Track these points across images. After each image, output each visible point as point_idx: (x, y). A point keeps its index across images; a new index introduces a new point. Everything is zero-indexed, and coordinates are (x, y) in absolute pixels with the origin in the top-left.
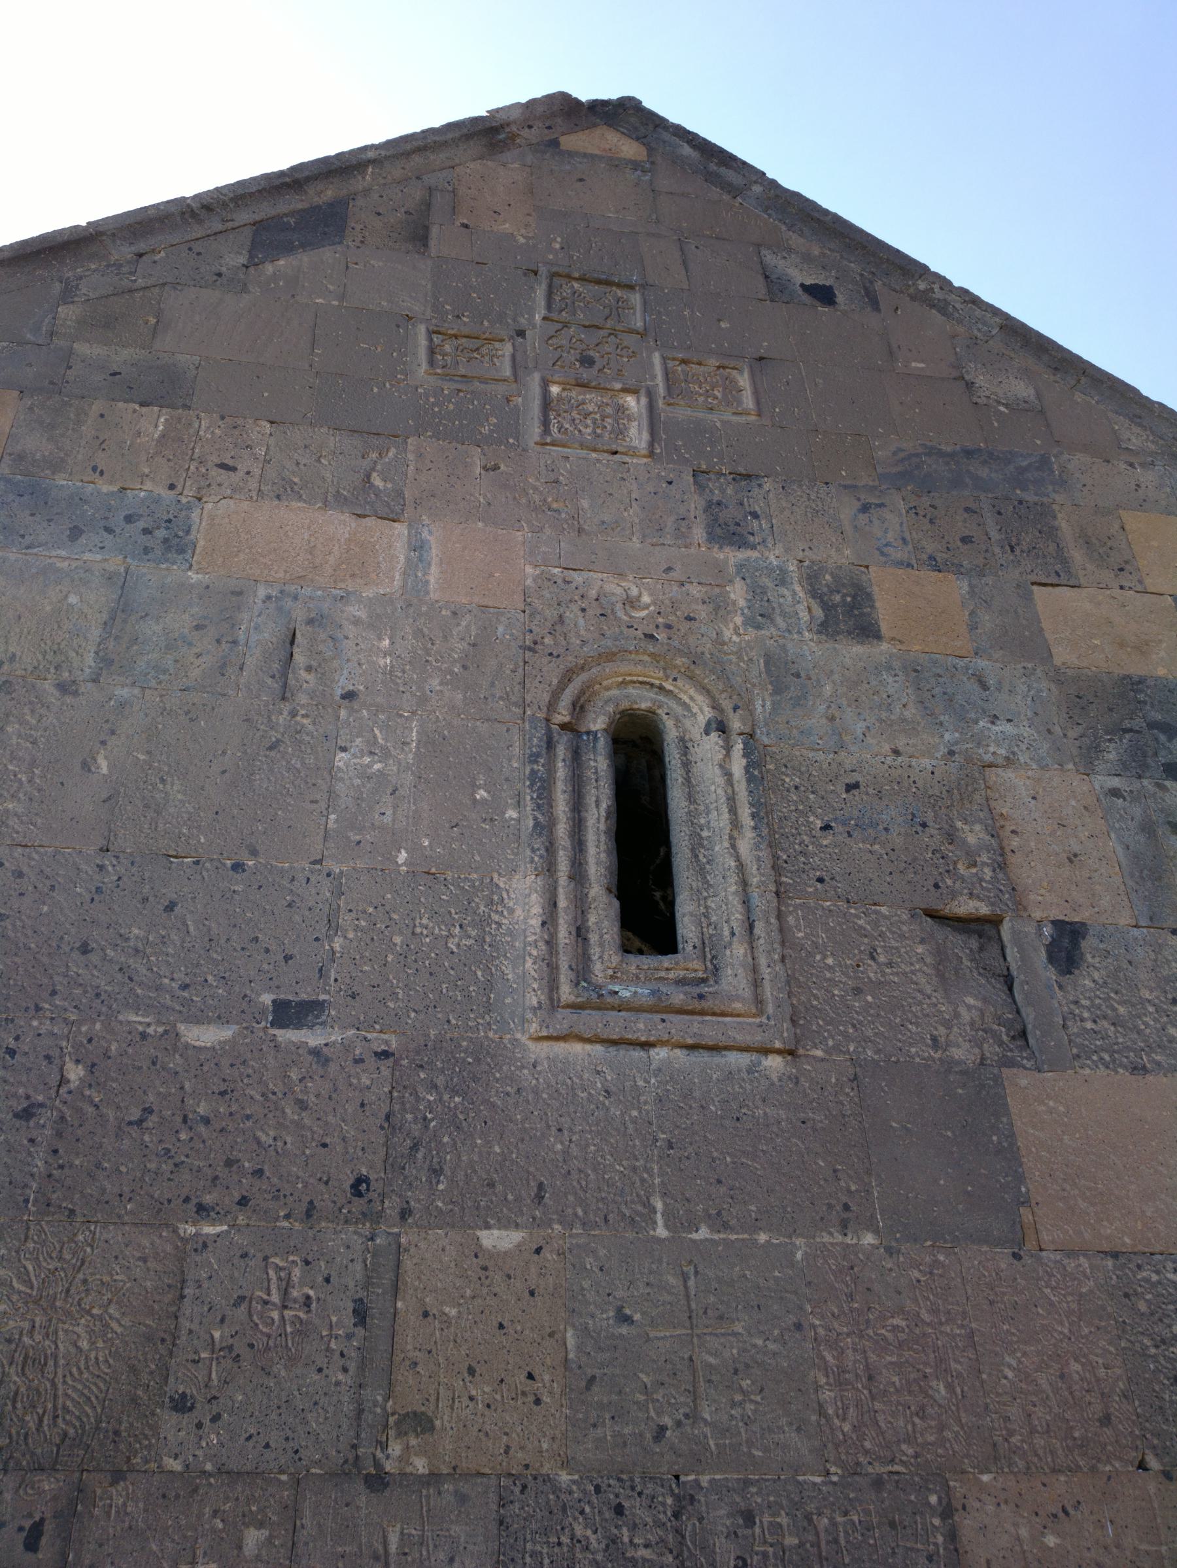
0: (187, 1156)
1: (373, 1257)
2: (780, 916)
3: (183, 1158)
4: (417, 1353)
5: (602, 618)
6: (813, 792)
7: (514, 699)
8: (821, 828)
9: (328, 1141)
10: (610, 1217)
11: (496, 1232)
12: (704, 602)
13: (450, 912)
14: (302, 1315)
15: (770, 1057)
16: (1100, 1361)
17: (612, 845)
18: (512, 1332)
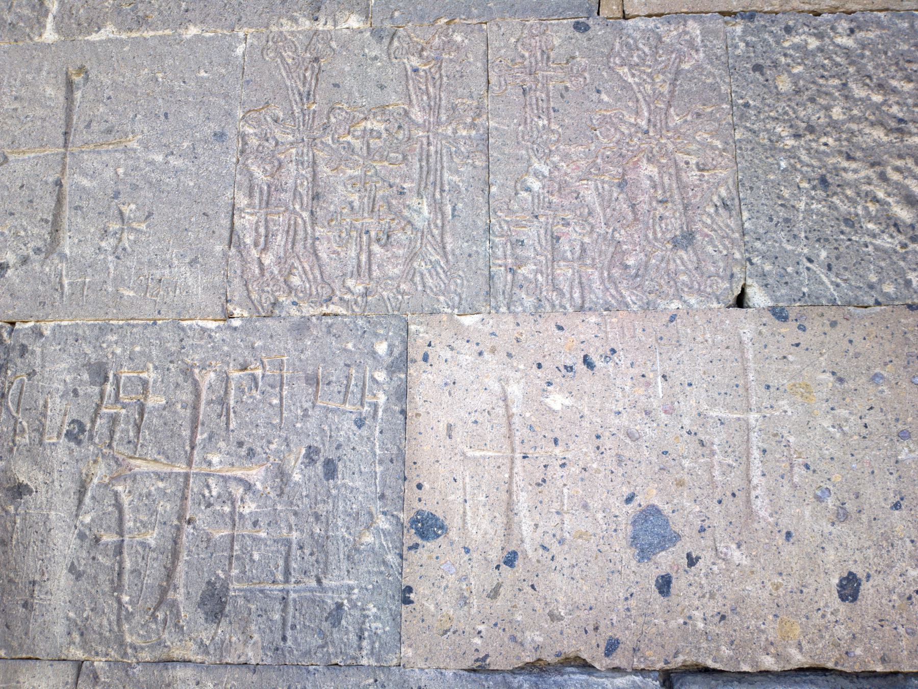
16: (693, 160)
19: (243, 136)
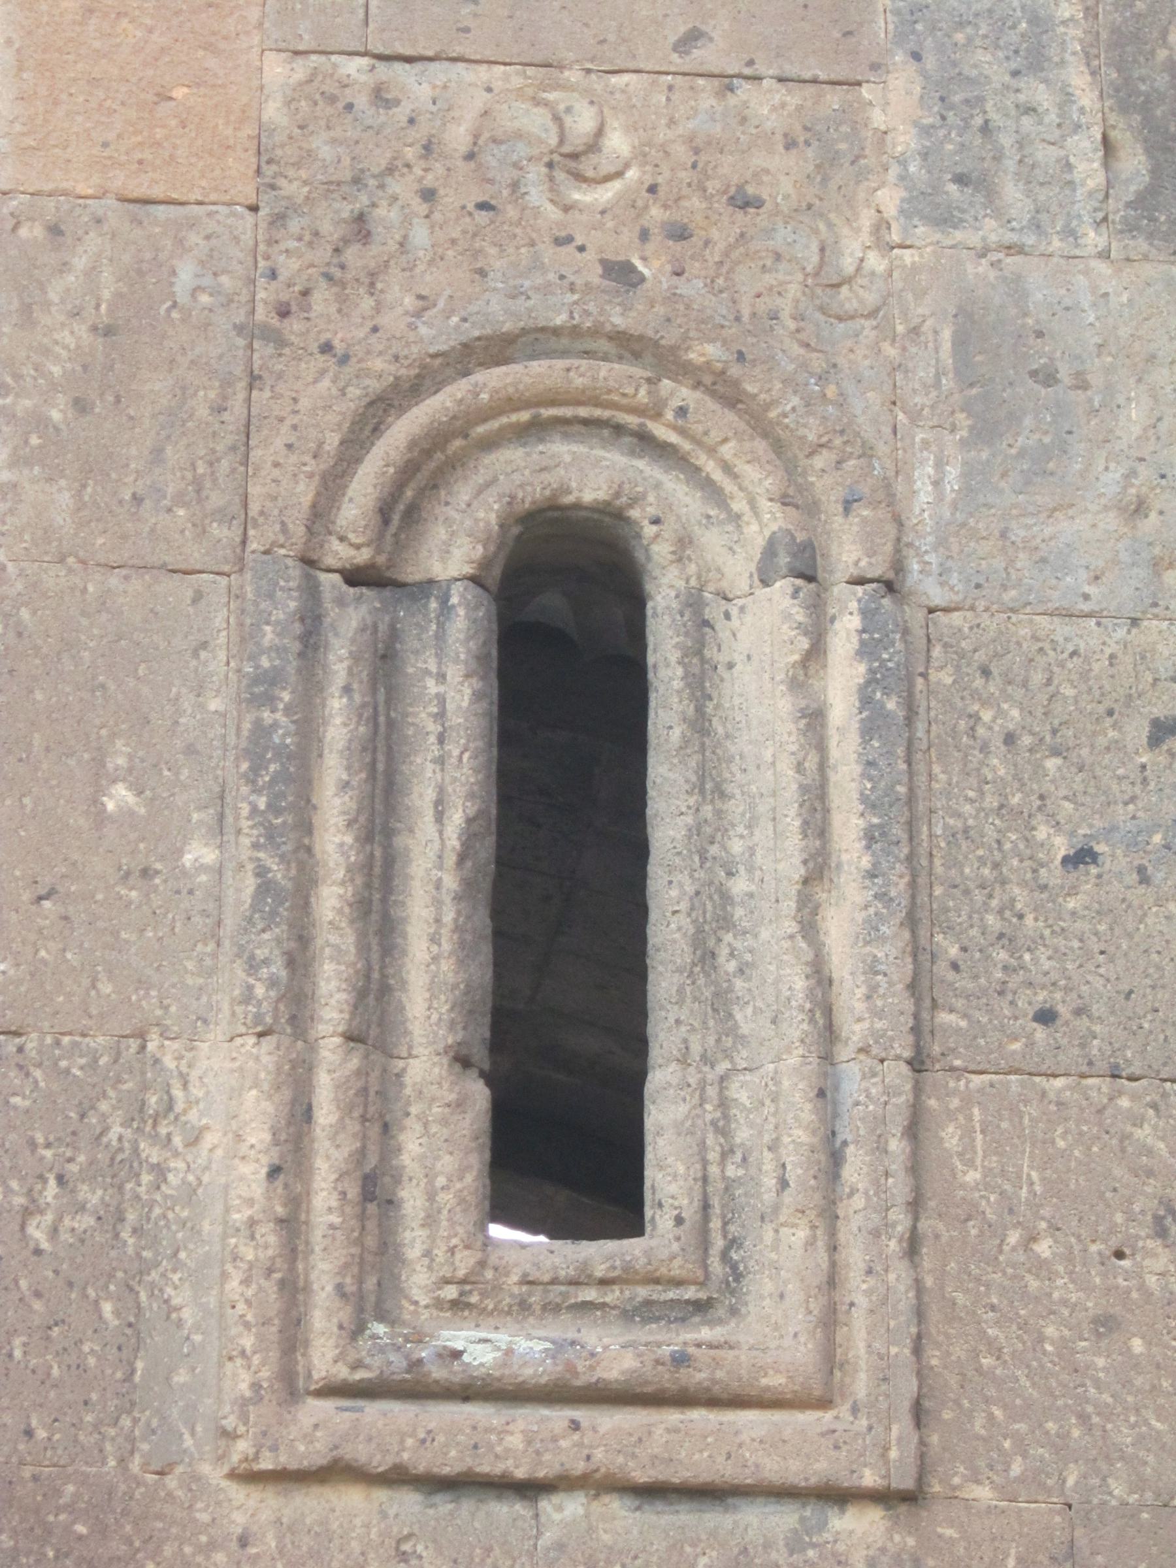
2: (914, 1129)
5: (482, 217)
6: (1055, 752)
7: (216, 499)
8: (1066, 860)
12: (791, 144)
13: (33, 1145)
17: (483, 920)
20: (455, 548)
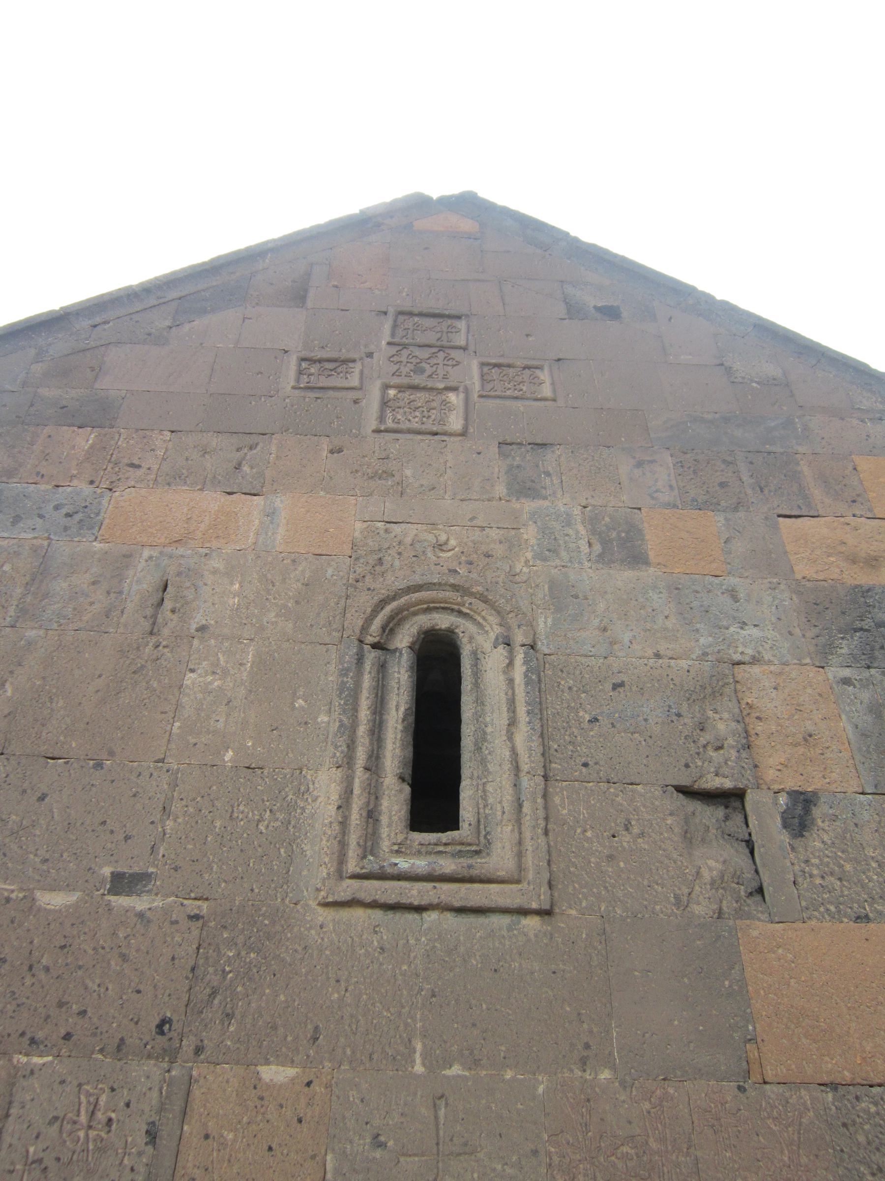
0: (28, 998)
1: (168, 1085)
2: (545, 796)
3: (24, 1000)
4: (195, 1170)
5: (414, 559)
6: (584, 692)
7: (335, 626)
8: (589, 721)
9: (141, 987)
10: (375, 1056)
11: (273, 1067)
12: (501, 542)
13: (263, 801)
14: (103, 1134)
15: (529, 918)
17: (410, 739)
18: (279, 1154)
19: (549, 1154)
20: (404, 639)
